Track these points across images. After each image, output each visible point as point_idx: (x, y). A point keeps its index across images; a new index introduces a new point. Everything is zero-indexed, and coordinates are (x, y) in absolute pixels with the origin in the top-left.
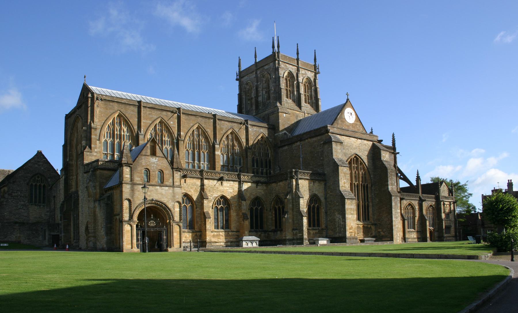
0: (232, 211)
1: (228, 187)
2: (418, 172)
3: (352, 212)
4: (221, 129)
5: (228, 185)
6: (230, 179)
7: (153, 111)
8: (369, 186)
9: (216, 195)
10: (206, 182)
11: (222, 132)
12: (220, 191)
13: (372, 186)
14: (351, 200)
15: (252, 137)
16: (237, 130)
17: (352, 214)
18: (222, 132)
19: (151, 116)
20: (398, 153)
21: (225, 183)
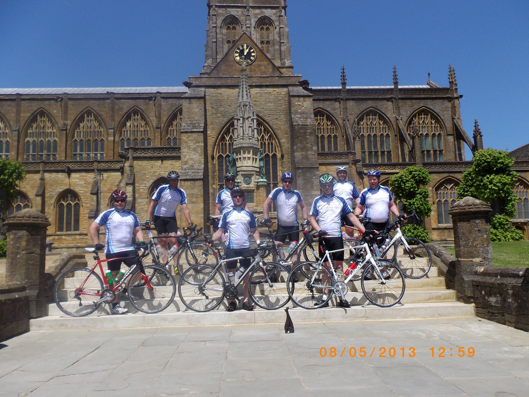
0: (81, 209)
1: (77, 178)
2: (476, 123)
3: (194, 200)
4: (121, 109)
5: (78, 176)
6: (82, 168)
7: (33, 102)
8: (279, 155)
9: (61, 190)
10: (47, 175)
11: (121, 113)
12: (66, 184)
13: (282, 156)
14: (192, 182)
15: (165, 113)
16: (143, 107)
17: (193, 203)
18: (121, 113)
19: (29, 108)
20: (461, 96)
21: (73, 175)
